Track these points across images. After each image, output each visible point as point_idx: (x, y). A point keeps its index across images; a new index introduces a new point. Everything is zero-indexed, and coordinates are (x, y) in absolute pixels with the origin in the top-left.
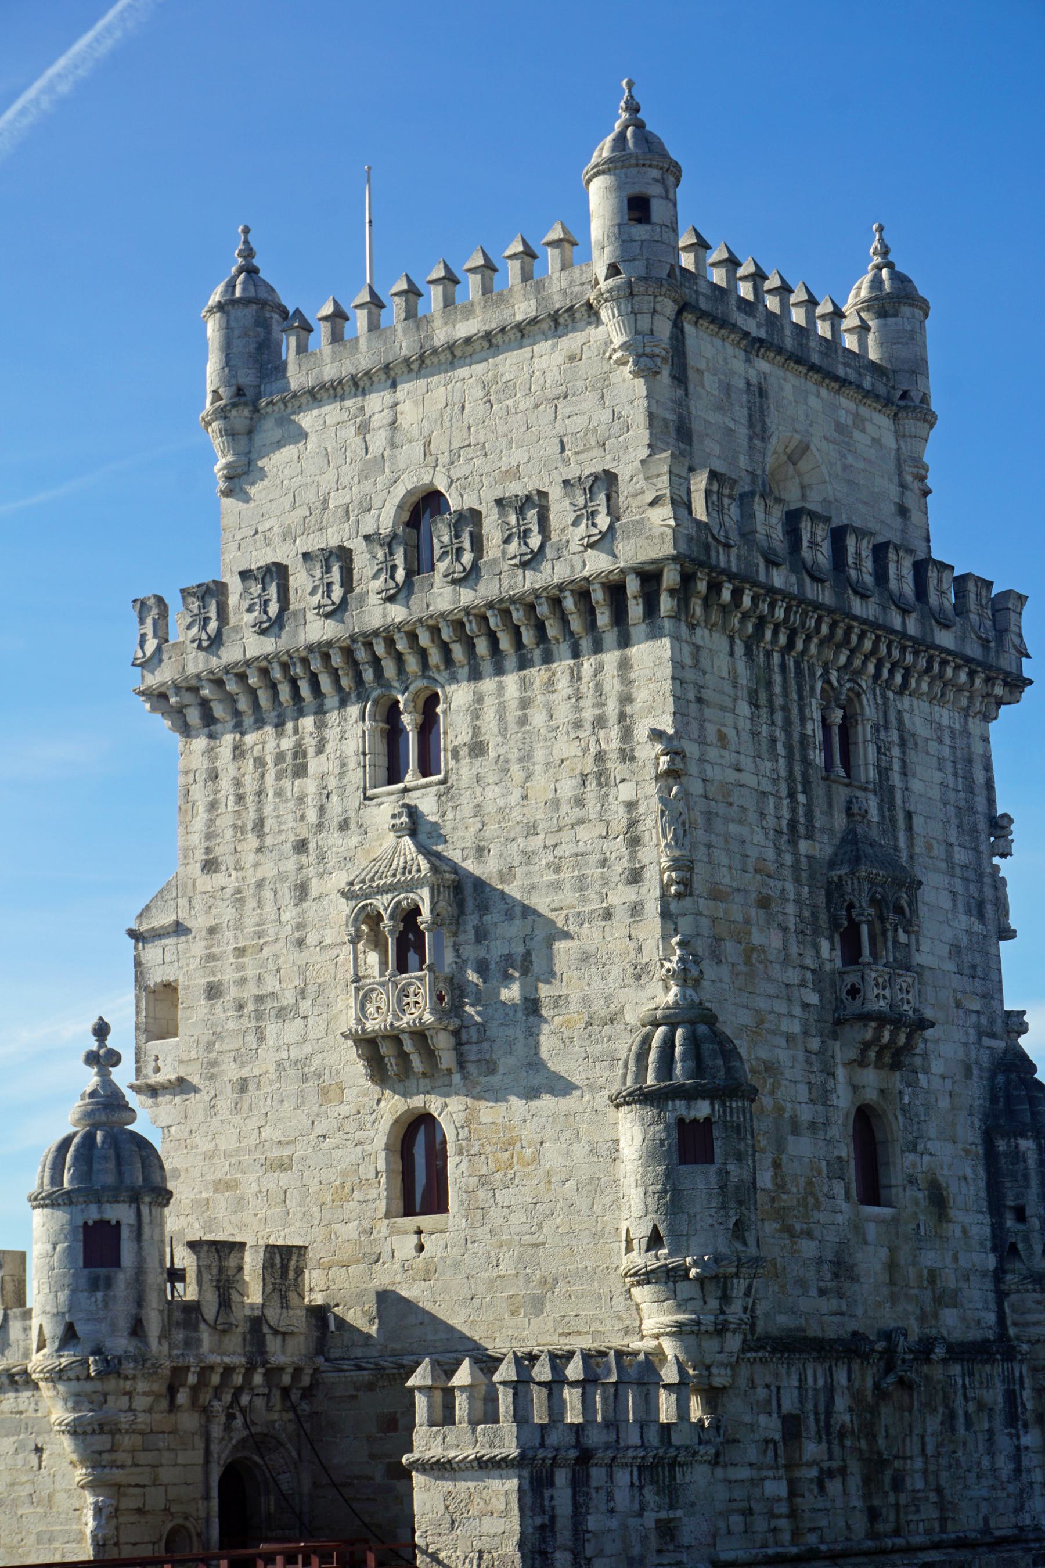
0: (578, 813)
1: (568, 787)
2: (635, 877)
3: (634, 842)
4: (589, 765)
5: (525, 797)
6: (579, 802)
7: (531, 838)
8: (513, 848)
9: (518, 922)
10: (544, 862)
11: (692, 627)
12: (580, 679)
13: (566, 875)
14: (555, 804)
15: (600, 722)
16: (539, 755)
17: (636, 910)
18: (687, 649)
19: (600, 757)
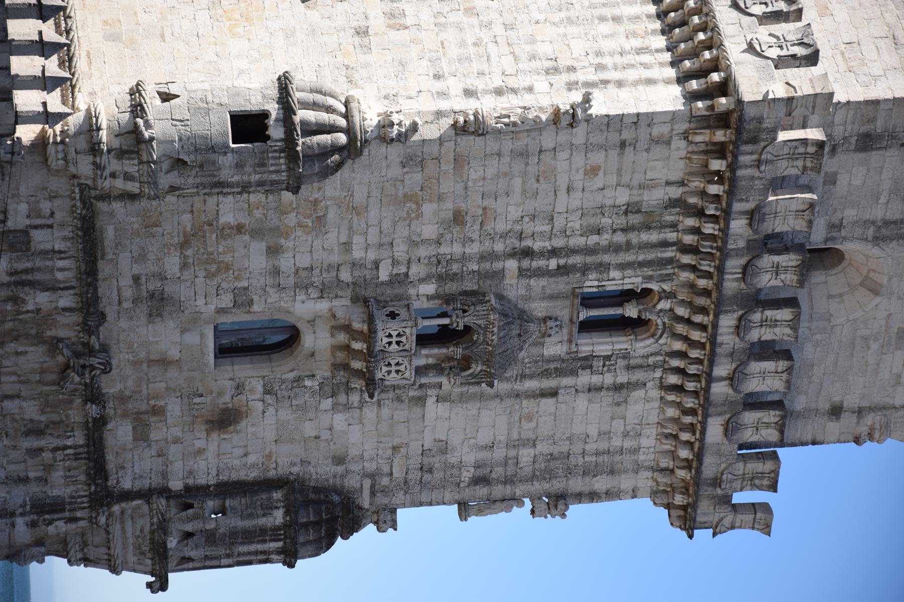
0: (524, 57)
1: (545, 49)
2: (469, 93)
3: (499, 92)
4: (563, 63)
5: (537, 22)
6: (533, 57)
7: (503, 27)
8: (494, 16)
9: (432, 19)
10: (483, 36)
11: (685, 135)
12: (638, 54)
13: (472, 50)
14: (532, 41)
15: (600, 67)
16: (573, 30)
17: (443, 95)
18: (665, 129)
19: (572, 69)
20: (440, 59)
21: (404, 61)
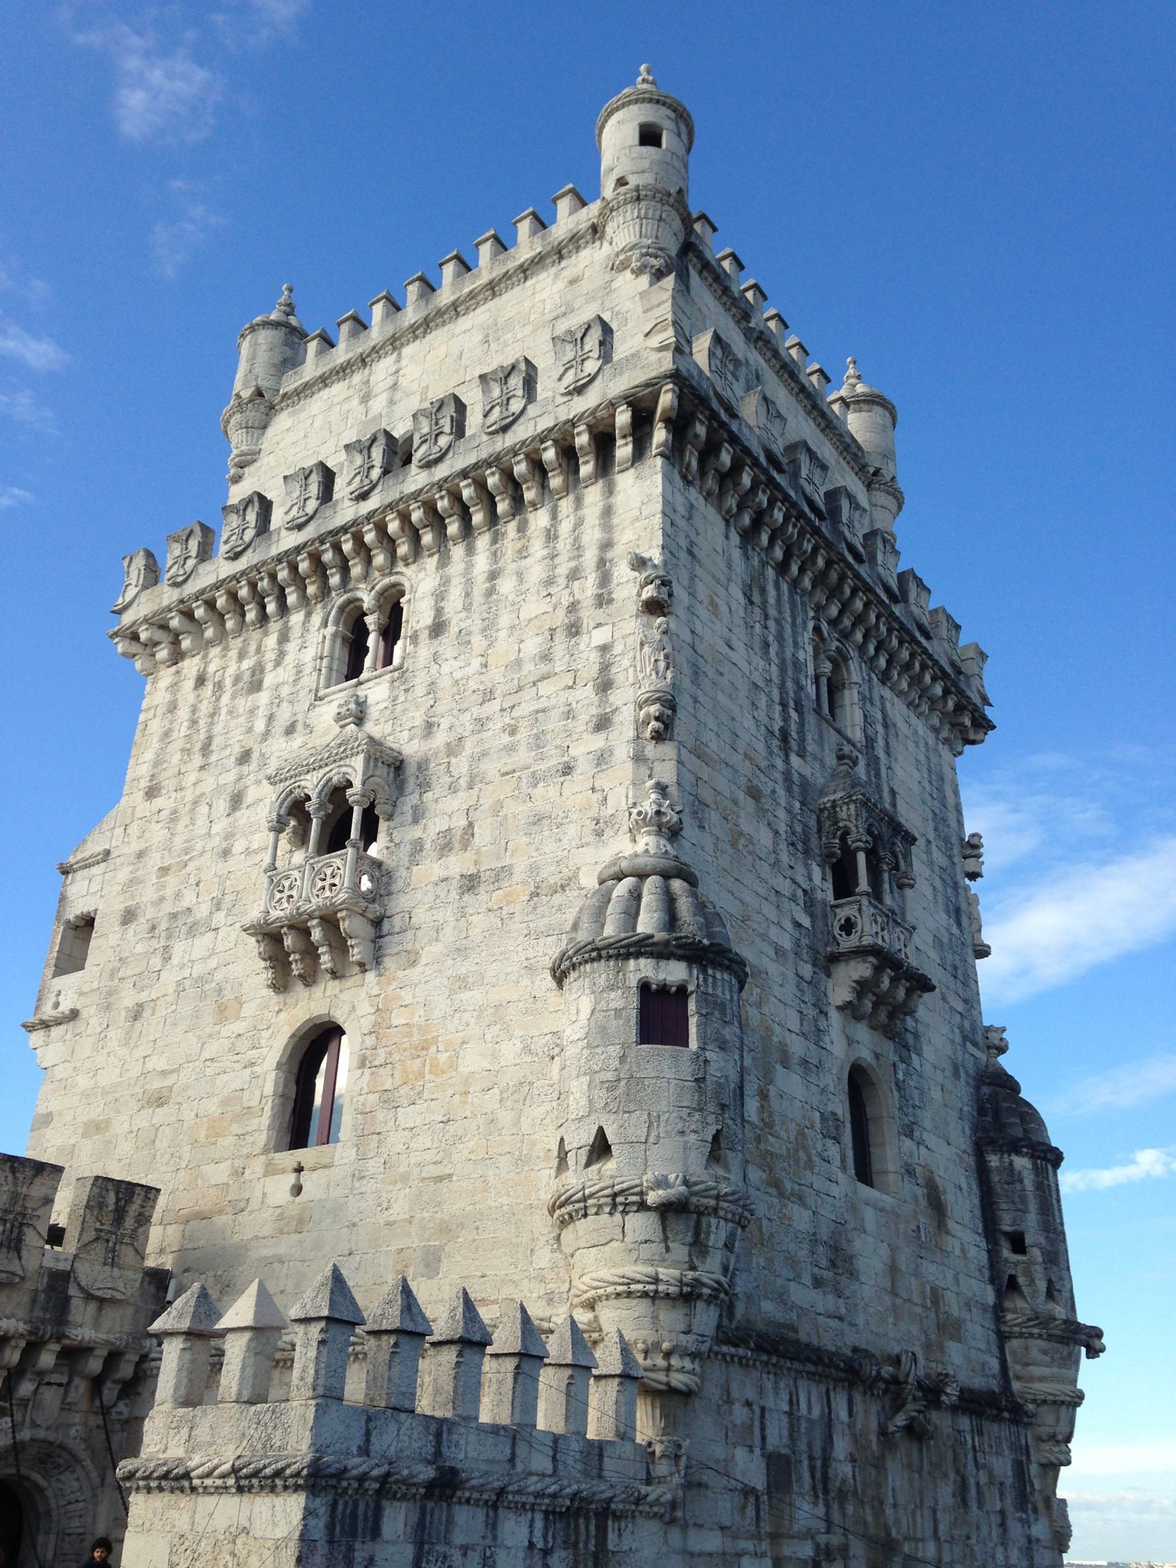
0: (544, 668)
6: (546, 657)
10: (499, 725)
20: (534, 772)
21: (531, 819)
